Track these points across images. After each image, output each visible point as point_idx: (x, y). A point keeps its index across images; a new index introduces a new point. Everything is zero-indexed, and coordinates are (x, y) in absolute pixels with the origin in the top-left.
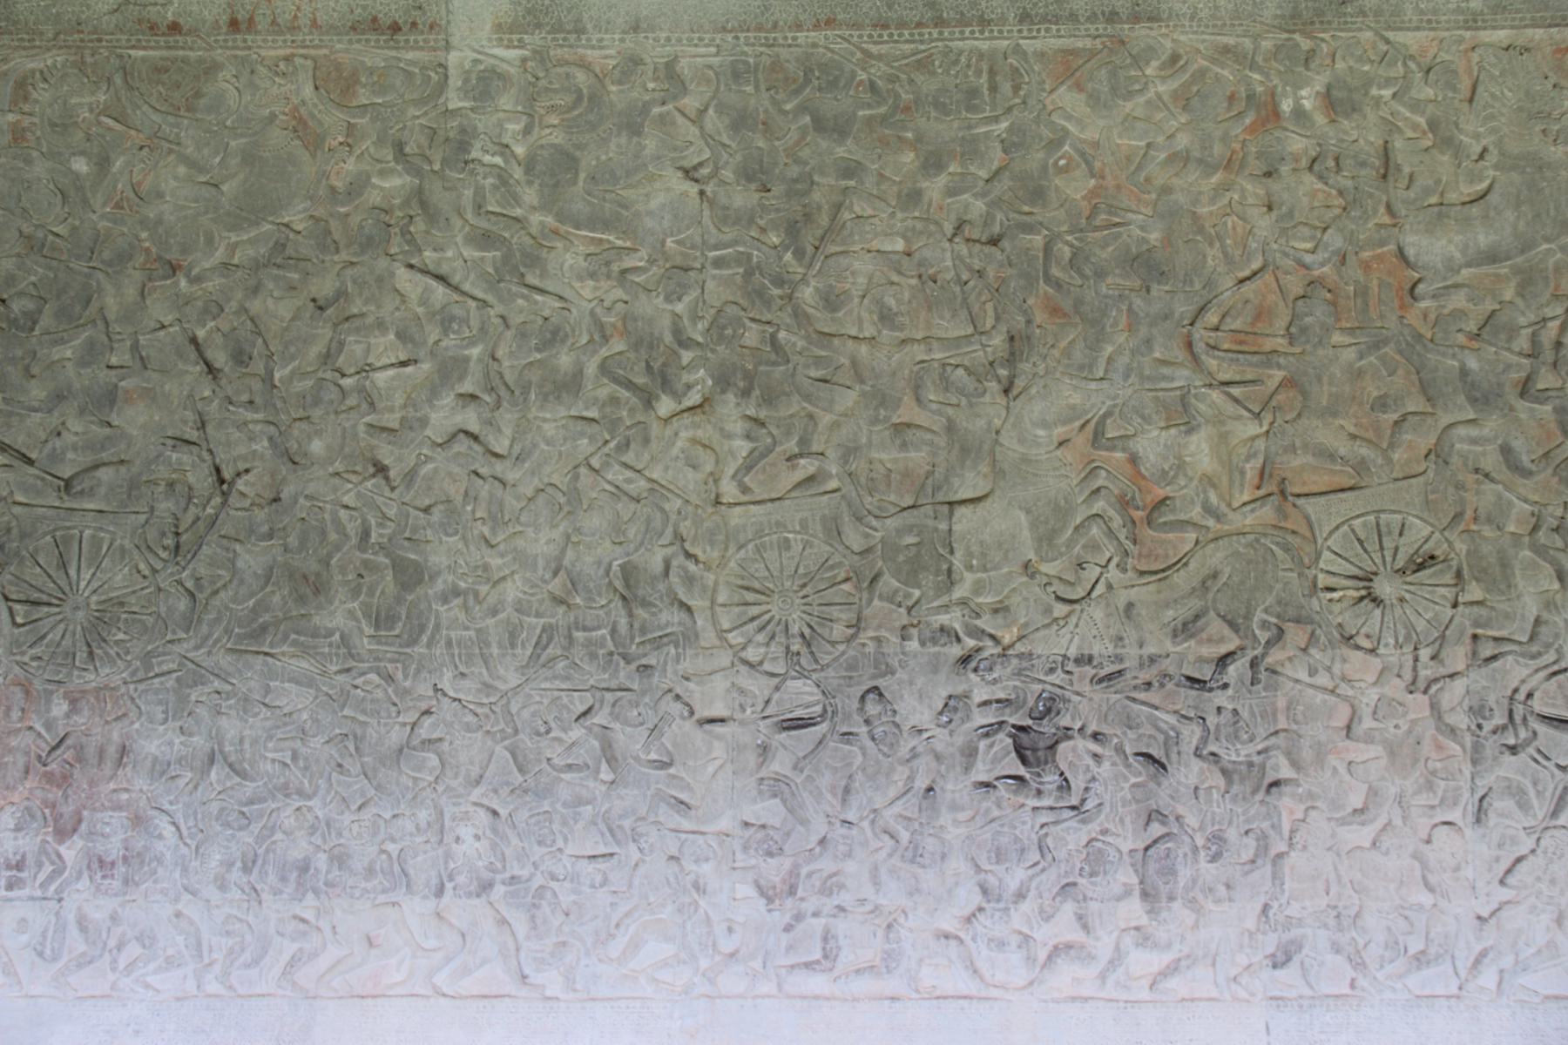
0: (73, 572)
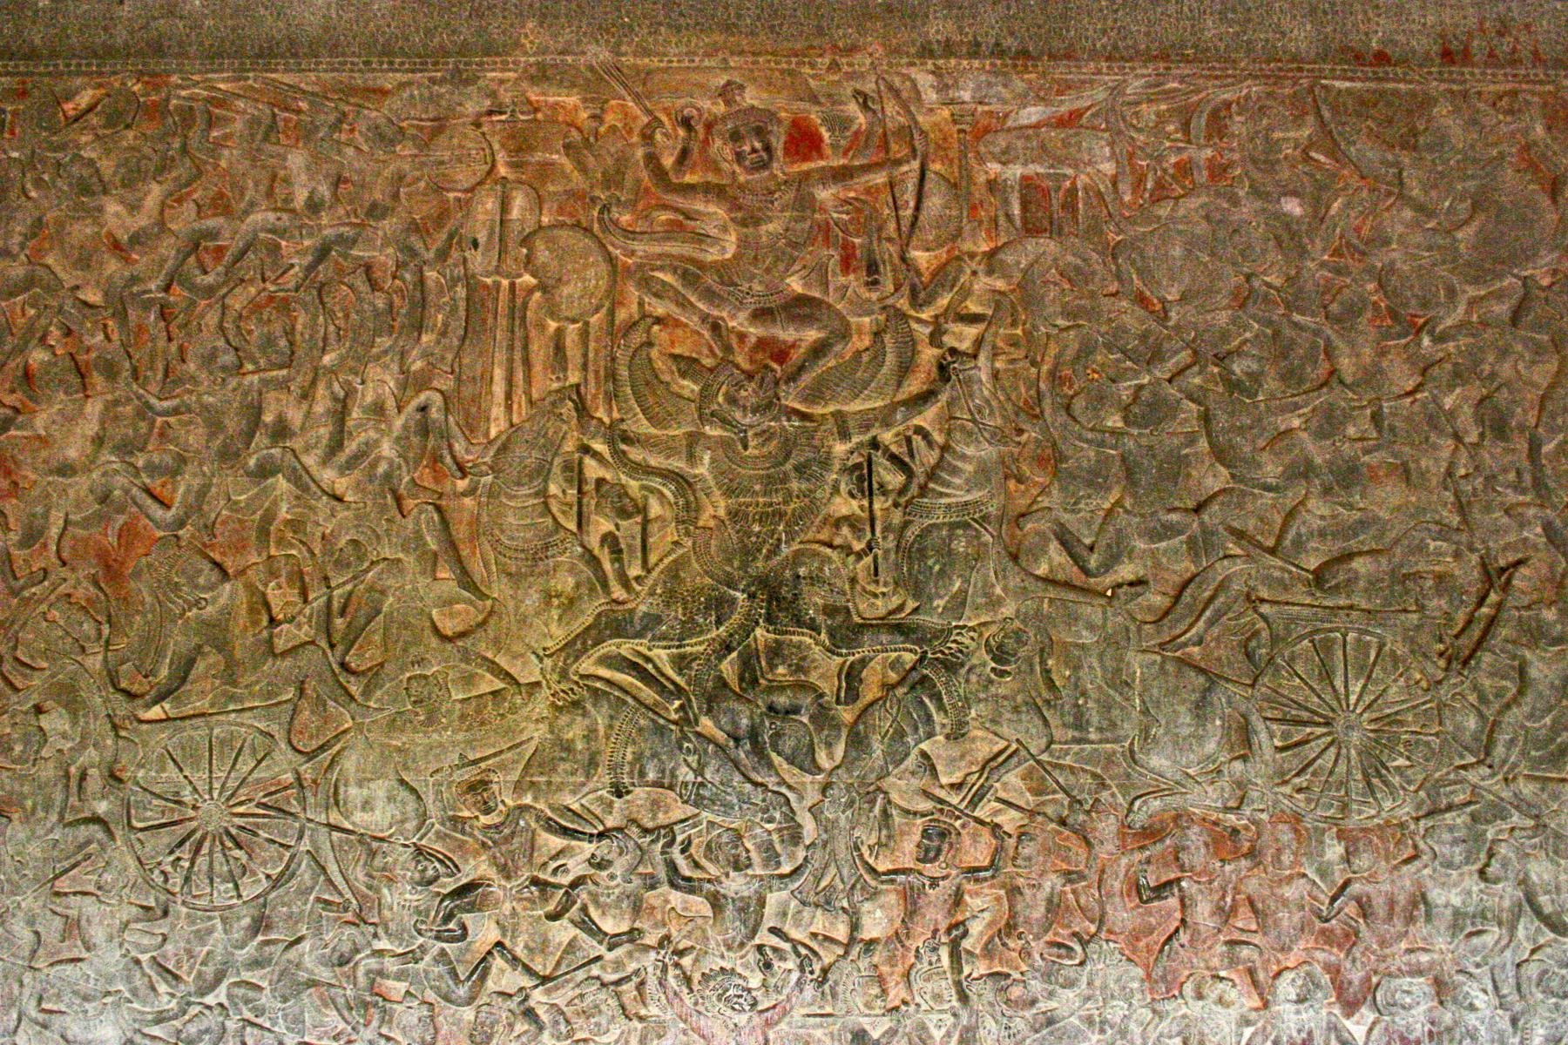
0: (1339, 683)
